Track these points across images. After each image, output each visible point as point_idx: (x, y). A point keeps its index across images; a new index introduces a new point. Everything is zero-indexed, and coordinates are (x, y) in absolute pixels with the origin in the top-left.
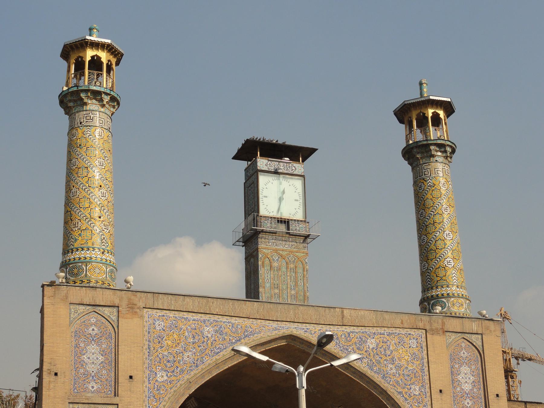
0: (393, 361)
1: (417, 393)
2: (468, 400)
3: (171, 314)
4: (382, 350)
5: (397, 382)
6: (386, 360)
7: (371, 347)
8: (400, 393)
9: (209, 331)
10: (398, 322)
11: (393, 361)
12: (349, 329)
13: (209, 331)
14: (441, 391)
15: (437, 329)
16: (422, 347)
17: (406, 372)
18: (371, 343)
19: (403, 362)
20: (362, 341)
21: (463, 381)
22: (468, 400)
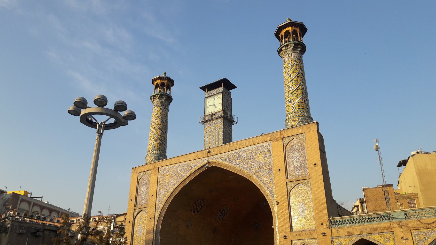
0: (254, 160)
1: (267, 174)
2: (298, 171)
3: (167, 167)
4: (249, 157)
5: (256, 171)
6: (251, 161)
7: (244, 157)
8: (258, 176)
9: (179, 170)
10: (257, 142)
11: (254, 161)
12: (233, 152)
13: (179, 170)
14: (279, 170)
15: (278, 138)
16: (270, 150)
17: (261, 165)
18: (244, 155)
19: (260, 160)
20: (240, 156)
21: (294, 161)
22: (298, 171)
